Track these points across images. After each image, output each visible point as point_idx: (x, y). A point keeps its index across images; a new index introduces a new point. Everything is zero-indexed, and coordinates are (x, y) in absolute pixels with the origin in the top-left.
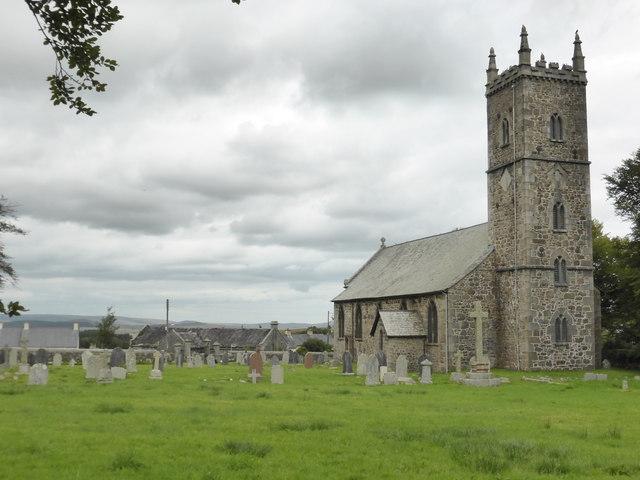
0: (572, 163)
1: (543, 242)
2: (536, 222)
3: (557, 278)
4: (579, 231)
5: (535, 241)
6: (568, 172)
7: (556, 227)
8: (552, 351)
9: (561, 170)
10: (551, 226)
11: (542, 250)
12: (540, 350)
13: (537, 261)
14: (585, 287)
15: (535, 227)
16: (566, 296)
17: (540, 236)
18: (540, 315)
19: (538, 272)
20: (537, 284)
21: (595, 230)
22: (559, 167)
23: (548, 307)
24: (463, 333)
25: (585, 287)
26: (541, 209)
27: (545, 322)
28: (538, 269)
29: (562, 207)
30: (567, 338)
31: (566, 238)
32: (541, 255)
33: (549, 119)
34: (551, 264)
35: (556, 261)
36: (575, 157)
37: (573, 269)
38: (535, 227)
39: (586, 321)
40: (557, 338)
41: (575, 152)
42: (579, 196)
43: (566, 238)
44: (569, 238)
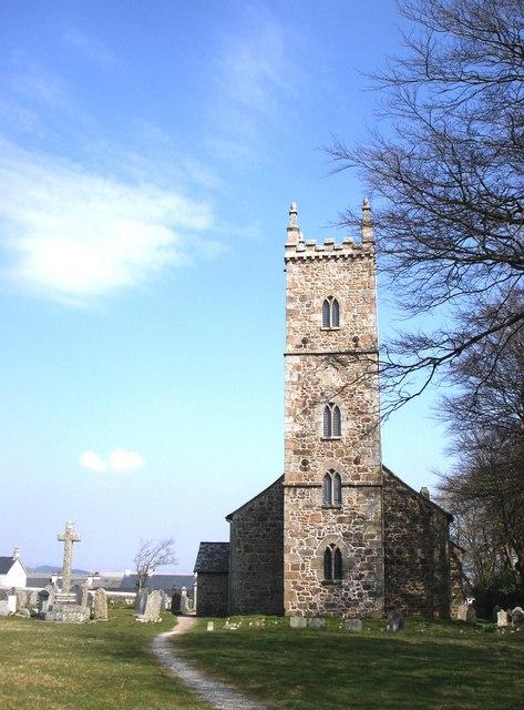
1: (308, 453)
2: (297, 428)
3: (328, 497)
5: (295, 452)
10: (321, 434)
11: (305, 463)
16: (341, 520)
18: (302, 544)
19: (299, 490)
27: (308, 553)
30: (340, 575)
34: (320, 480)
35: (327, 476)
37: (351, 486)
39: (369, 552)
40: (327, 574)
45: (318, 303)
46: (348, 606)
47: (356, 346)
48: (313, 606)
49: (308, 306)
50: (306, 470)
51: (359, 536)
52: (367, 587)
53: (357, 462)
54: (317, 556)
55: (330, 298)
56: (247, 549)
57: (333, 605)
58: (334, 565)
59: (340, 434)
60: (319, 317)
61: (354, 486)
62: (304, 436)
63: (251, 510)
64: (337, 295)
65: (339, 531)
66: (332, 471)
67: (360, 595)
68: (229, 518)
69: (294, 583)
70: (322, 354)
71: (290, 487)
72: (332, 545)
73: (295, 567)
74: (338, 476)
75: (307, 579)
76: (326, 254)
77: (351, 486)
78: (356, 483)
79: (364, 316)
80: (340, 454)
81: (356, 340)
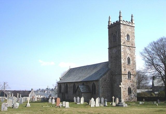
7: (128, 63)
9: (130, 49)
11: (125, 69)
16: (131, 82)
22: (129, 48)
26: (125, 58)
27: (125, 88)
28: (124, 74)
30: (131, 93)
33: (126, 35)
35: (128, 73)
37: (132, 75)
39: (135, 88)
40: (129, 93)
41: (132, 44)
45: (126, 35)
46: (132, 99)
47: (132, 45)
48: (127, 100)
50: (125, 71)
51: (133, 85)
52: (135, 95)
53: (133, 70)
54: (127, 89)
55: (128, 34)
56: (103, 87)
57: (130, 99)
58: (130, 91)
59: (130, 64)
60: (126, 38)
64: (129, 34)
65: (131, 83)
66: (129, 71)
67: (134, 97)
70: (127, 46)
71: (123, 74)
72: (129, 87)
73: (124, 92)
74: (130, 73)
76: (128, 24)
77: (132, 75)
78: (133, 74)
79: (133, 39)
80: (130, 68)
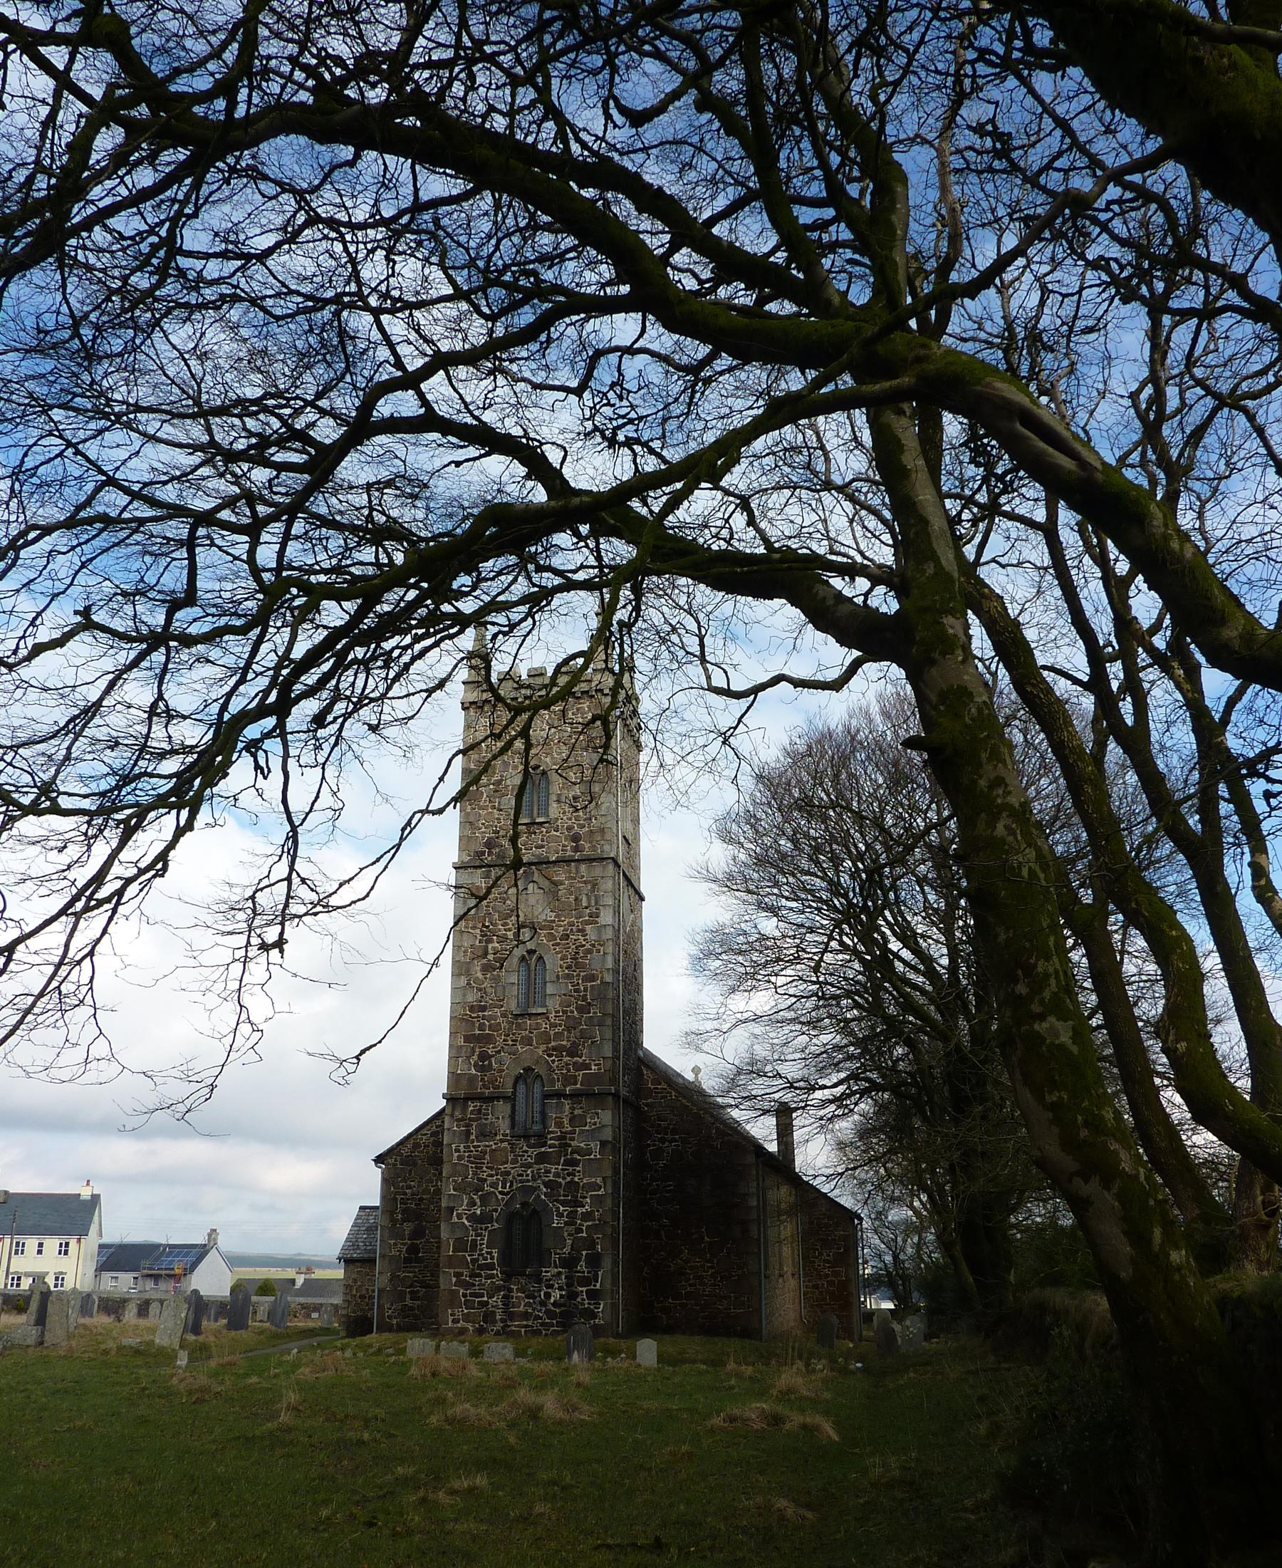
0: (568, 861)
1: (488, 1039)
2: (472, 998)
4: (581, 1010)
5: (468, 1039)
6: (555, 884)
8: (499, 1289)
11: (484, 1056)
12: (467, 1285)
13: (472, 1079)
14: (592, 1134)
15: (472, 1009)
16: (542, 1158)
17: (481, 1028)
18: (472, 1203)
20: (468, 1133)
21: (616, 998)
23: (494, 1185)
24: (413, 1249)
25: (592, 1134)
26: (485, 969)
27: (484, 1219)
29: (541, 958)
30: (542, 1258)
31: (544, 1026)
32: (482, 1069)
36: (576, 849)
37: (559, 1095)
38: (472, 1009)
39: (587, 1216)
42: (582, 931)
43: (544, 1026)
44: (553, 1026)
49: (499, 783)
61: (565, 1096)
62: (483, 1009)
63: (416, 1146)
68: (379, 1160)
69: (458, 1275)
75: (481, 1267)
81: (576, 838)
